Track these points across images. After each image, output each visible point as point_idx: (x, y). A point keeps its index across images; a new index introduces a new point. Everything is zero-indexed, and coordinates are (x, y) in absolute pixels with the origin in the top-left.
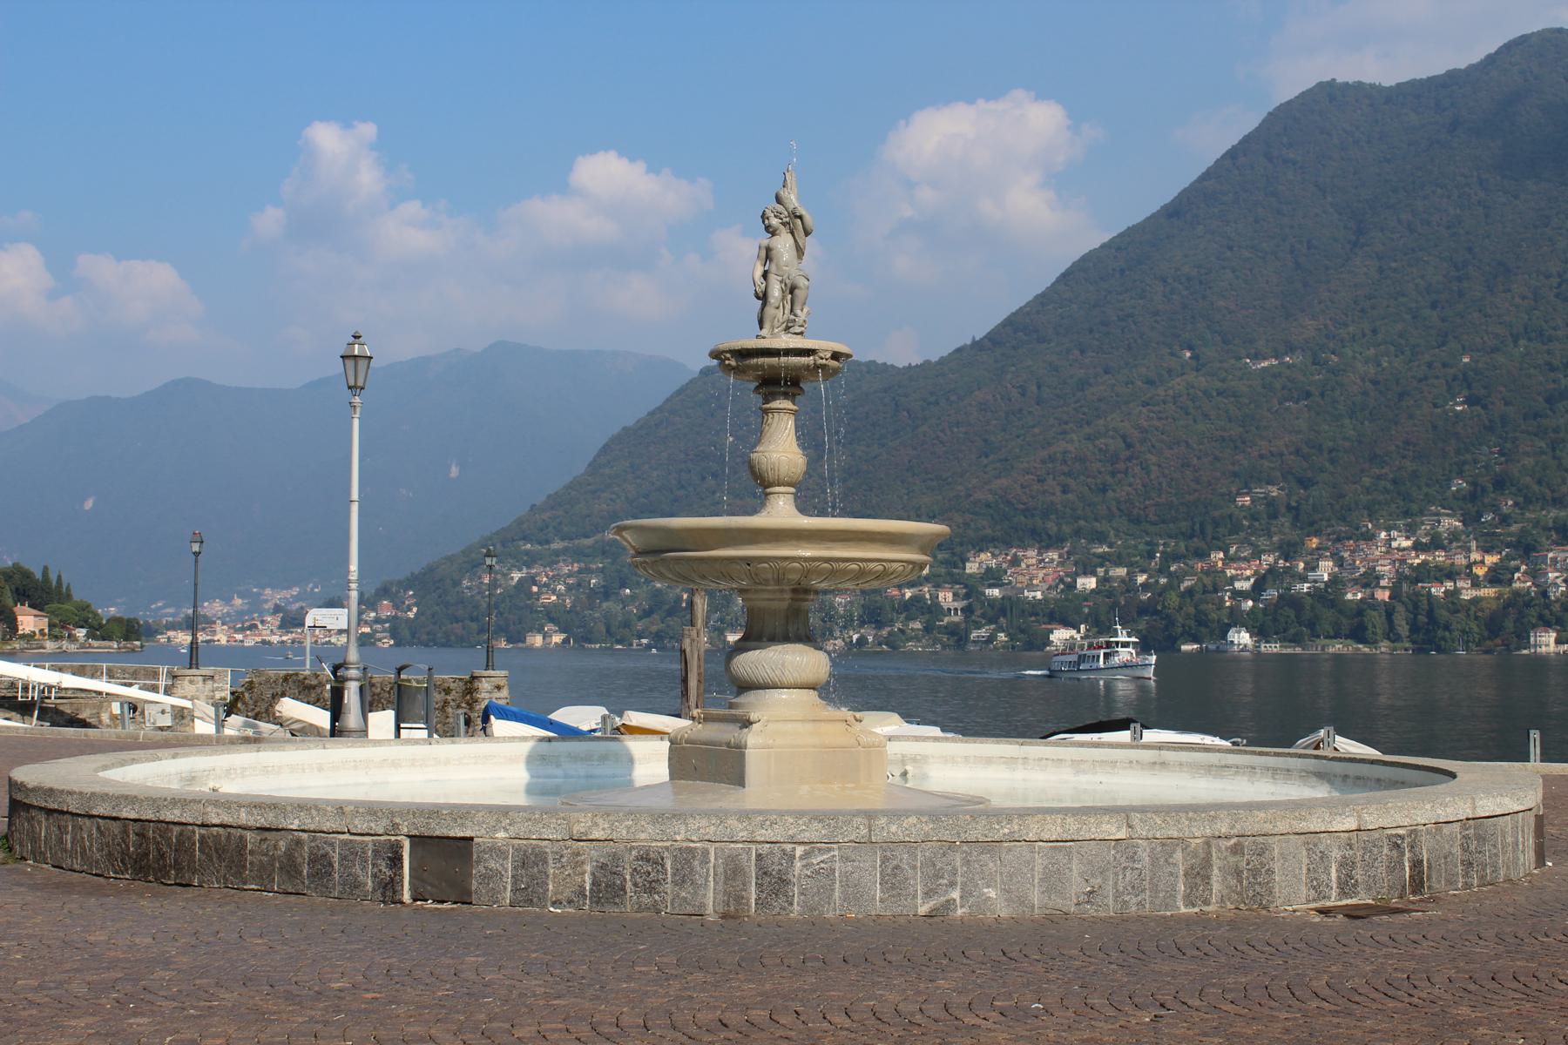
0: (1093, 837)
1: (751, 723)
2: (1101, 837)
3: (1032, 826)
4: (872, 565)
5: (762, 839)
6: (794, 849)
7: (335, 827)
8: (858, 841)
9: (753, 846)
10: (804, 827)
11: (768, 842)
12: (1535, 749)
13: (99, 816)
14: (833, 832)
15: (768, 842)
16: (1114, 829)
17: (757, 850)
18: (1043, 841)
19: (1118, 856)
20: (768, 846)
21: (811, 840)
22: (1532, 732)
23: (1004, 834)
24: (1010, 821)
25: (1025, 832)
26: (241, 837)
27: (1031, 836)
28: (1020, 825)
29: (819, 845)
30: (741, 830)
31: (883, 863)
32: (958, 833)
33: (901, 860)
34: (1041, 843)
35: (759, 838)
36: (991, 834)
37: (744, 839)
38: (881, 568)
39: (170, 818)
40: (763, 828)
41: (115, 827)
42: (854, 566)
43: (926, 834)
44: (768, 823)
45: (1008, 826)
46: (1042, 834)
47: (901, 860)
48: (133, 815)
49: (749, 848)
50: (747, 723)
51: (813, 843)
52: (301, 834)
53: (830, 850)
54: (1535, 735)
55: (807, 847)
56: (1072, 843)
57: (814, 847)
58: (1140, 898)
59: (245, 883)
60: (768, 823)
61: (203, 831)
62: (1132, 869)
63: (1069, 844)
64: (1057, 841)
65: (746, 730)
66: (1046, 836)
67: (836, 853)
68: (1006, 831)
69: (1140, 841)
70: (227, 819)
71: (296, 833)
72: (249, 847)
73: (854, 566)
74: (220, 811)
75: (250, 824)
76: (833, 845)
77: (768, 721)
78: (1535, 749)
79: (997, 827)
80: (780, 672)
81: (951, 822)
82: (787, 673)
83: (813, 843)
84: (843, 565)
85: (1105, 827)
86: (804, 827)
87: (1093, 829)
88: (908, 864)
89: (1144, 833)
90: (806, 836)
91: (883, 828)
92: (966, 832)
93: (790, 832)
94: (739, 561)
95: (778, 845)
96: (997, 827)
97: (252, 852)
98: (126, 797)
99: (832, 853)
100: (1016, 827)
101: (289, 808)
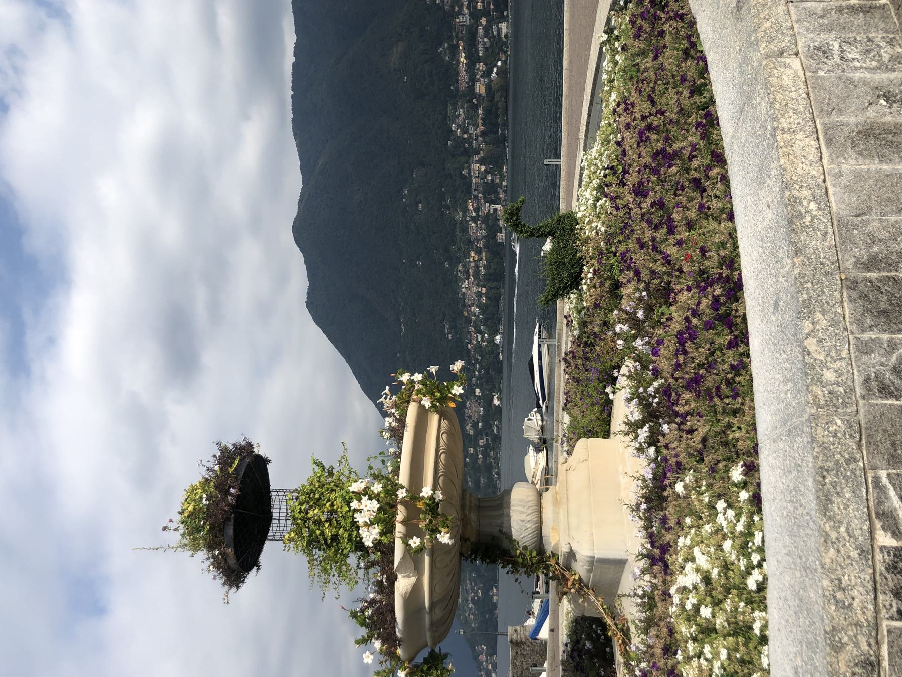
0: (804, 95)
1: (571, 550)
2: (803, 86)
3: (800, 171)
4: (442, 443)
5: (871, 607)
6: (882, 548)
8: (858, 435)
9: (885, 624)
10: (843, 529)
11: (876, 598)
12: (554, 162)
14: (845, 477)
15: (876, 598)
16: (788, 71)
17: (892, 618)
18: (821, 158)
19: (826, 68)
20: (881, 597)
21: (865, 517)
22: (545, 163)
23: (819, 209)
24: (796, 200)
25: (811, 181)
27: (815, 171)
28: (801, 187)
29: (871, 504)
30: (857, 645)
31: (891, 395)
32: (827, 274)
33: (882, 364)
34: (825, 161)
35: (870, 614)
36: (822, 227)
37: (872, 641)
38: (445, 436)
40: (850, 605)
42: (443, 457)
43: (834, 324)
44: (839, 595)
45: (805, 203)
46: (811, 158)
47: (882, 364)
49: (889, 632)
50: (571, 554)
51: (869, 515)
53: (877, 481)
54: (546, 162)
55: (878, 524)
56: (818, 122)
57: (877, 514)
58: (883, 44)
60: (839, 595)
62: (842, 52)
63: (819, 127)
64: (818, 139)
65: (577, 556)
66: (813, 155)
67: (883, 474)
68: (813, 206)
69: (800, 44)
73: (443, 457)
76: (870, 480)
77: (569, 535)
78: (554, 162)
79: (808, 218)
80: (528, 523)
81: (809, 285)
82: (529, 518)
83: (869, 515)
84: (441, 467)
85: (787, 81)
86: (843, 529)
87: (794, 95)
88: (889, 353)
89: (788, 38)
90: (859, 526)
91: (830, 393)
92: (822, 264)
93: (854, 554)
94: (435, 557)
95: (878, 578)
96: (808, 218)
99: (885, 481)
100: (805, 192)
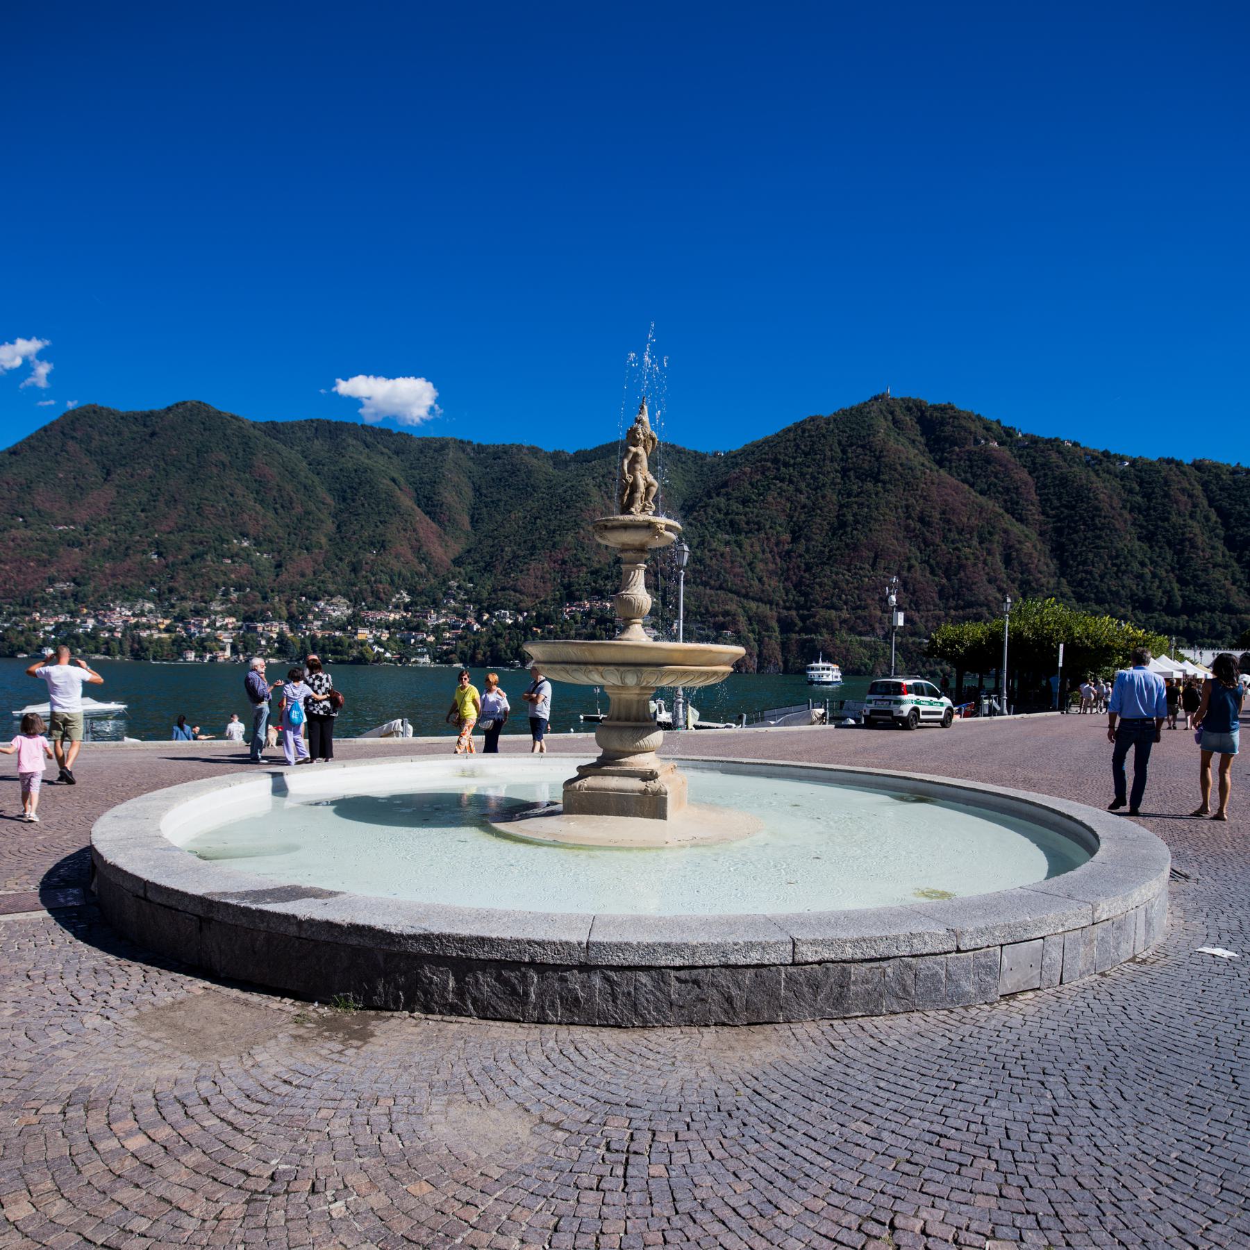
7: (946, 948)
13: (611, 968)
26: (844, 969)
39: (742, 961)
41: (643, 978)
48: (678, 962)
52: (910, 959)
59: (848, 1012)
61: (791, 969)
70: (827, 955)
71: (906, 959)
72: (853, 978)
74: (820, 949)
75: (856, 957)
97: (855, 983)
98: (667, 945)
101: (902, 938)
